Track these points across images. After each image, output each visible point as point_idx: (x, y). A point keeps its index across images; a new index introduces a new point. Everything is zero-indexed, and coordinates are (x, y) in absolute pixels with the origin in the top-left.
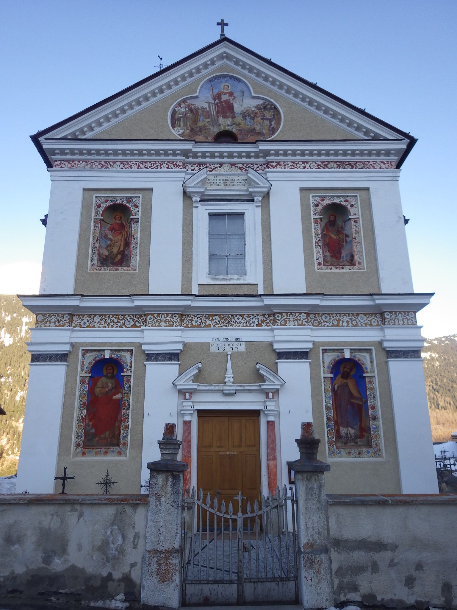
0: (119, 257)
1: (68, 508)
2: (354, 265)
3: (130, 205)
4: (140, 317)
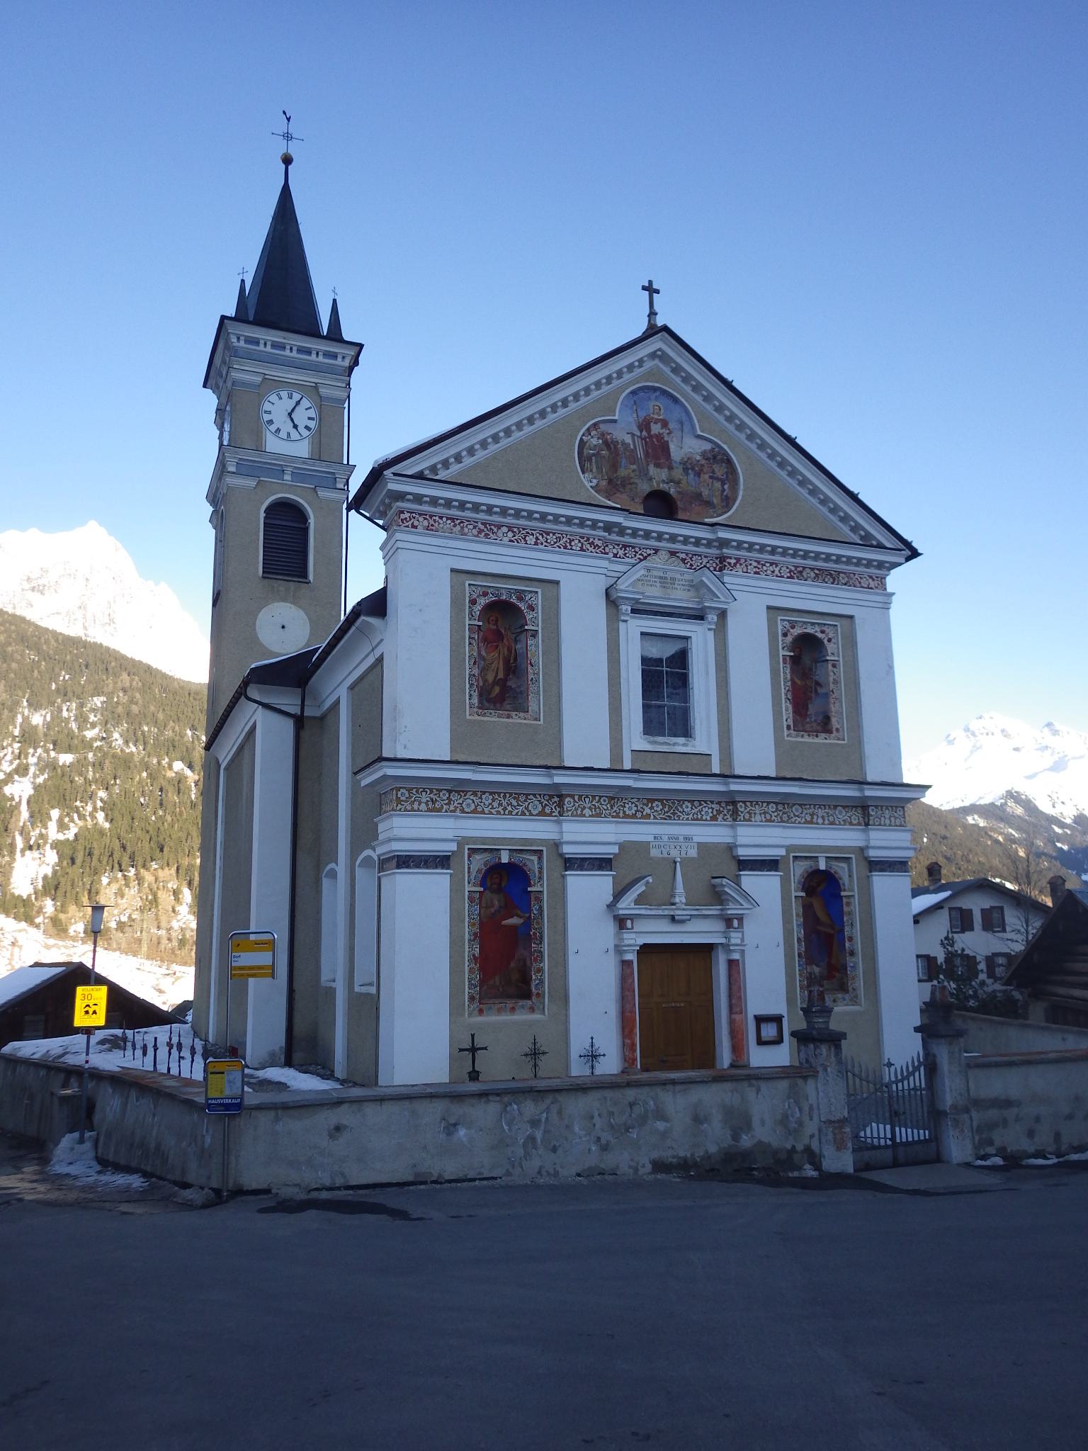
0: (497, 689)
1: (745, 1084)
2: (831, 732)
3: (522, 606)
4: (556, 801)
